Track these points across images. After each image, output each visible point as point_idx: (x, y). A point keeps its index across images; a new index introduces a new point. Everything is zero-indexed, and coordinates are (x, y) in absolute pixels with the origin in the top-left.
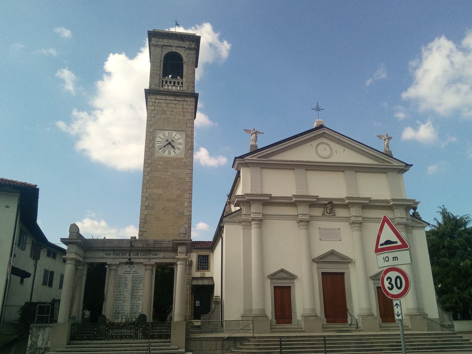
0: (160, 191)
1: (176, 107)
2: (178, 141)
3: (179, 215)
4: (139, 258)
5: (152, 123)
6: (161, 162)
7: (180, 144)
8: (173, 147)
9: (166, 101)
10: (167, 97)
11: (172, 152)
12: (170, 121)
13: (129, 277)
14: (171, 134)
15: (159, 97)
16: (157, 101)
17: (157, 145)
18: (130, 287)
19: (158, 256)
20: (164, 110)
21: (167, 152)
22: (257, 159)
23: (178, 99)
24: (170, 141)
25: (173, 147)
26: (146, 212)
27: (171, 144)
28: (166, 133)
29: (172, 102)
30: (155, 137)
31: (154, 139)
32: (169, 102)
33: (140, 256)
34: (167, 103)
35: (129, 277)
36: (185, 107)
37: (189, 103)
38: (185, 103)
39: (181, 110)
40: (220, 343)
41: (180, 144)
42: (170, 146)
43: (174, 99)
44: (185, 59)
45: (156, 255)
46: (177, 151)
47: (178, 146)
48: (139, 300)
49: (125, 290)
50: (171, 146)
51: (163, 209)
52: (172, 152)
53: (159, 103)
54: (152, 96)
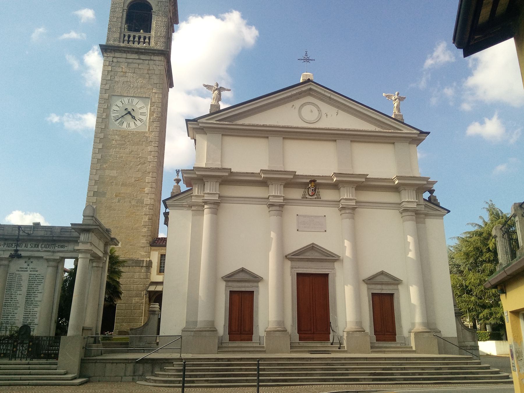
0: (114, 173)
1: (139, 67)
2: (141, 111)
3: (137, 203)
4: (39, 251)
5: (107, 87)
6: (116, 136)
7: (142, 114)
8: (133, 118)
9: (128, 60)
10: (128, 54)
11: (132, 126)
12: (132, 86)
13: (25, 276)
14: (132, 102)
15: (117, 55)
16: (115, 60)
17: (113, 115)
18: (24, 289)
19: (66, 249)
20: (123, 71)
21: (125, 125)
22: (215, 122)
23: (142, 57)
24: (130, 110)
25: (133, 118)
26: (94, 199)
27: (131, 114)
28: (126, 100)
29: (135, 61)
30: (111, 105)
31: (109, 108)
32: (130, 61)
33: (40, 248)
34: (128, 63)
35: (25, 276)
36: (151, 68)
37: (157, 63)
38: (151, 63)
39: (146, 72)
40: (130, 367)
41: (142, 114)
42: (129, 117)
43: (137, 57)
44: (155, 8)
45: (62, 247)
46: (138, 123)
47: (141, 117)
48: (36, 306)
49: (19, 292)
50: (130, 117)
51: (116, 196)
52: (132, 126)
53: (118, 62)
54: (109, 54)
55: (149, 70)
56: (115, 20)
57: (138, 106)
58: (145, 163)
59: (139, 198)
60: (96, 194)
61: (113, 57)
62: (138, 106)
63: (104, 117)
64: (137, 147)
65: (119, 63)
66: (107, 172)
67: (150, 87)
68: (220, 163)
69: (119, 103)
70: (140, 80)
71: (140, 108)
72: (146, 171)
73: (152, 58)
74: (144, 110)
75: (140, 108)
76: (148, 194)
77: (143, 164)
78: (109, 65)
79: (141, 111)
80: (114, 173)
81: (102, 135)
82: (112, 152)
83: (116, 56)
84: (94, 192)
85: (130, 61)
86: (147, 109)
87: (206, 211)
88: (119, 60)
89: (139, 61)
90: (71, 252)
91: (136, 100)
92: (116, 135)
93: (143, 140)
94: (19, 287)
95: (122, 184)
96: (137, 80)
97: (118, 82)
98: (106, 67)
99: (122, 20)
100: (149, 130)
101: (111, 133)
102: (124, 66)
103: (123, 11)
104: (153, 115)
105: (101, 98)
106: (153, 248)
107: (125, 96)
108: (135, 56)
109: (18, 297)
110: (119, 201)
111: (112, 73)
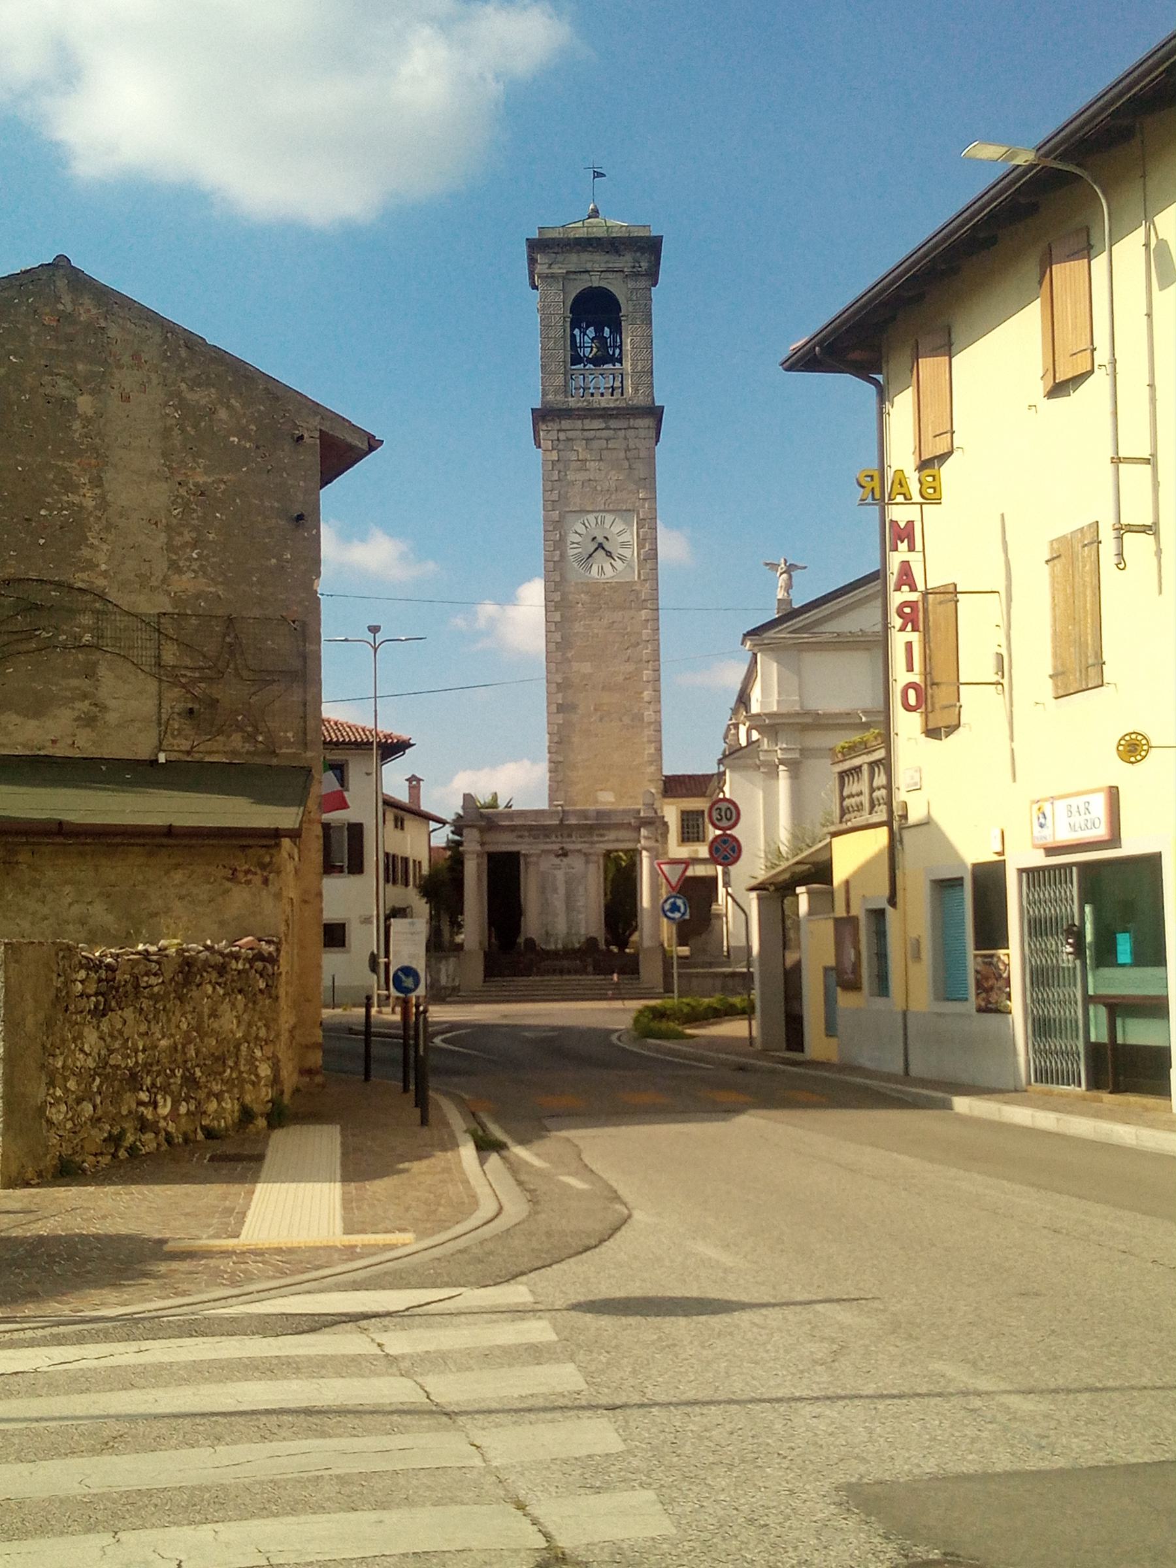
0: (586, 668)
1: (610, 446)
2: (621, 539)
3: (632, 720)
4: (574, 842)
5: (554, 496)
6: (582, 595)
7: (624, 545)
8: (609, 554)
9: (585, 433)
10: (587, 421)
11: (608, 568)
12: (599, 488)
13: (560, 875)
14: (603, 522)
15: (566, 424)
16: (562, 436)
17: (571, 552)
18: (562, 890)
19: (606, 838)
20: (580, 458)
21: (595, 568)
22: (788, 636)
23: (613, 424)
24: (600, 539)
25: (609, 554)
26: (560, 719)
27: (603, 548)
28: (591, 518)
29: (599, 434)
30: (565, 533)
31: (562, 539)
32: (591, 434)
33: (574, 839)
34: (587, 440)
35: (560, 875)
36: (632, 446)
37: (642, 433)
38: (631, 433)
39: (622, 455)
40: (718, 983)
41: (624, 545)
42: (601, 552)
43: (603, 425)
44: (622, 300)
45: (602, 835)
46: (618, 564)
47: (621, 551)
48: (579, 912)
49: (555, 896)
50: (603, 553)
51: (595, 710)
52: (608, 568)
53: (568, 439)
54: (550, 424)
55: (627, 450)
56: (551, 345)
57: (616, 529)
58: (638, 644)
59: (636, 711)
60: (561, 708)
61: (558, 431)
62: (616, 529)
63: (556, 559)
64: (620, 613)
65: (570, 443)
66: (576, 666)
67: (632, 487)
68: (797, 698)
69: (580, 528)
70: (614, 475)
71: (620, 534)
72: (641, 660)
73: (631, 424)
74: (625, 537)
75: (620, 534)
76: (650, 703)
77: (635, 647)
78: (553, 449)
79: (621, 539)
80: (586, 668)
81: (557, 597)
82: (578, 627)
83: (563, 428)
84: (558, 705)
85: (591, 434)
86: (632, 534)
87: (781, 774)
88: (570, 434)
89: (605, 433)
90: (614, 841)
91: (609, 518)
92: (583, 592)
93: (632, 598)
94: (555, 890)
95: (603, 688)
96: (607, 474)
97: (573, 483)
98: (548, 453)
99: (565, 341)
100: (639, 577)
101: (572, 589)
102: (579, 446)
103: (565, 321)
104: (644, 547)
105: (546, 521)
106: (667, 800)
107: (589, 512)
108: (598, 424)
109: (556, 903)
110: (601, 720)
111: (560, 466)
